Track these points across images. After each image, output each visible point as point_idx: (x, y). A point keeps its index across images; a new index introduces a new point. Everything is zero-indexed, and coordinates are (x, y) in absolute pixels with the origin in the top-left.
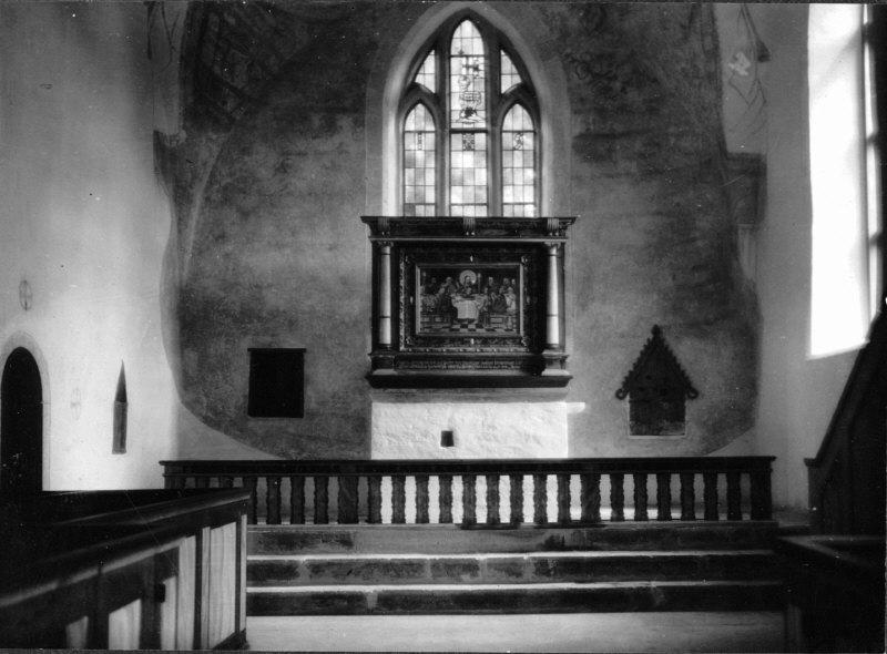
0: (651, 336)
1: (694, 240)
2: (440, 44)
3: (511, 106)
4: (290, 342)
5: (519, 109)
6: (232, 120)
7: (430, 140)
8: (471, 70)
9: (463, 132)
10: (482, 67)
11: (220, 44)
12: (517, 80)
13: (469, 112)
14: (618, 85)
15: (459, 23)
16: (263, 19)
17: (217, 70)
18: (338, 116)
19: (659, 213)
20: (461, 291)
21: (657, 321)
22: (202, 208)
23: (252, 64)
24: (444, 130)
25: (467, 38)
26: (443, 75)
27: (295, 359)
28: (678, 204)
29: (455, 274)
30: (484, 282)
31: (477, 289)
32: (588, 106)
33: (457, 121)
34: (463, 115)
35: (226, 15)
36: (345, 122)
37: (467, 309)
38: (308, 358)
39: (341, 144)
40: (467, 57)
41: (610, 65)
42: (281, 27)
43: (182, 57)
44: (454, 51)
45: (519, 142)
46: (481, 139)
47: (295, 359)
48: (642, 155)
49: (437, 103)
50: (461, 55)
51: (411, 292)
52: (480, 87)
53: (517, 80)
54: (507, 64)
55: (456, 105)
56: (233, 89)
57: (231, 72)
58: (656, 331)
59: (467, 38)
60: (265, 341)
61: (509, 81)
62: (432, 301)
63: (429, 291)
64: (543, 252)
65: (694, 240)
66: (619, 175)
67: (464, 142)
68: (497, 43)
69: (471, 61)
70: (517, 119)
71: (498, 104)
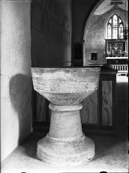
2: (112, 18)
5: (121, 25)
7: (111, 29)
13: (115, 25)
20: (115, 47)
25: (115, 17)
26: (112, 21)
27: (96, 54)
29: (115, 45)
30: (118, 45)
31: (117, 46)
36: (101, 28)
37: (116, 48)
38: (97, 54)
44: (114, 18)
46: (117, 29)
49: (112, 25)
51: (110, 47)
52: (117, 22)
55: (114, 25)
59: (115, 17)
61: (120, 21)
62: (112, 48)
63: (112, 47)
64: (125, 42)
68: (119, 18)
71: (119, 24)
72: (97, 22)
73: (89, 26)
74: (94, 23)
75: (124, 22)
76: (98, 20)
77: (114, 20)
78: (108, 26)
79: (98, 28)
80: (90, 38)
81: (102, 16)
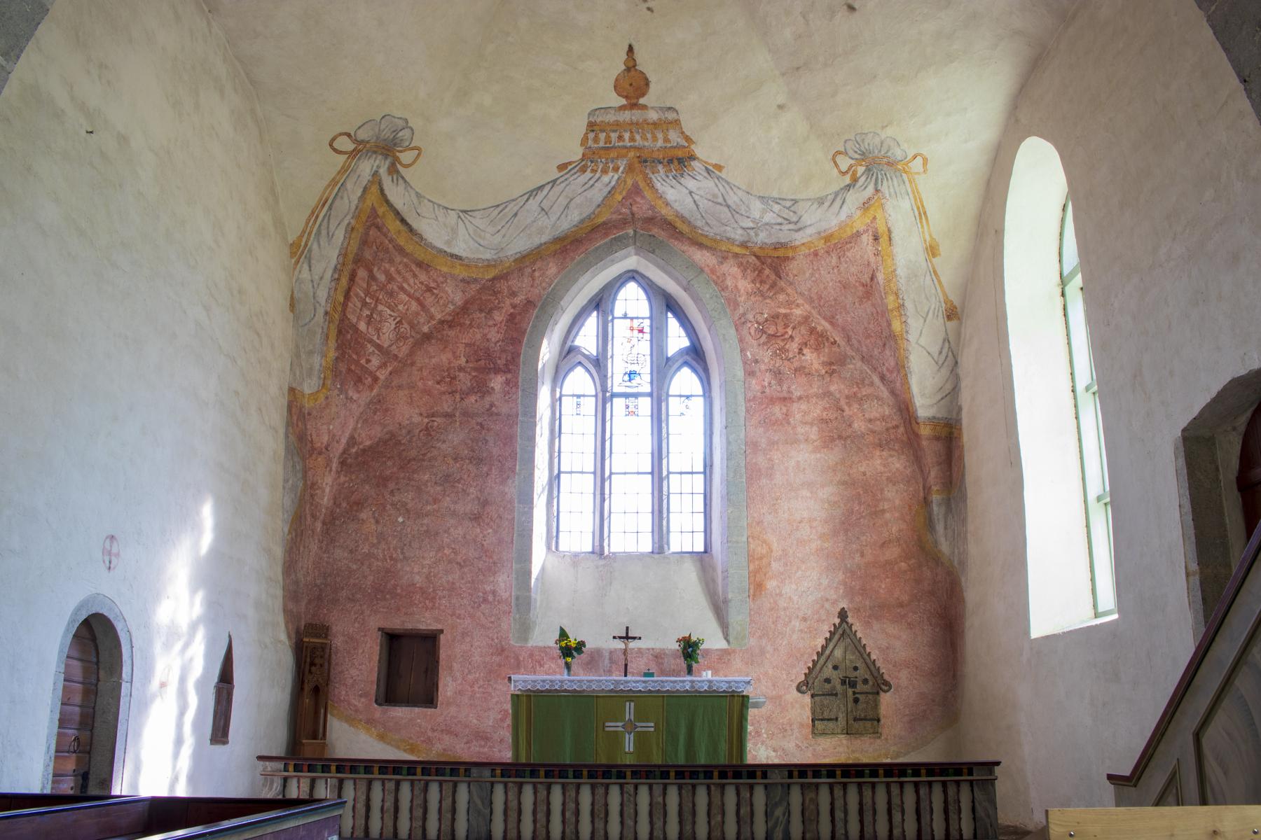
0: (837, 621)
1: (883, 511)
2: (601, 303)
3: (679, 369)
4: (424, 622)
5: (686, 371)
6: (376, 379)
7: (589, 405)
8: (636, 332)
9: (626, 396)
10: (647, 329)
11: (368, 300)
12: (685, 343)
13: (631, 375)
14: (794, 346)
15: (623, 284)
16: (415, 276)
17: (362, 326)
18: (492, 376)
19: (844, 483)
21: (844, 604)
22: (338, 472)
23: (400, 322)
24: (605, 397)
26: (604, 337)
27: (430, 640)
28: (864, 474)
32: (763, 367)
33: (617, 383)
34: (627, 378)
35: (375, 269)
36: (497, 382)
39: (492, 406)
40: (632, 319)
41: (786, 326)
42: (432, 285)
43: (326, 313)
44: (618, 312)
45: (687, 407)
46: (645, 404)
47: (430, 640)
48: (823, 421)
50: (625, 317)
52: (644, 347)
53: (685, 343)
54: (673, 323)
55: (617, 369)
56: (379, 347)
57: (378, 330)
58: (843, 615)
60: (397, 623)
61: (677, 339)
65: (883, 511)
66: (796, 441)
67: (627, 407)
69: (636, 323)
70: (685, 381)
71: (663, 368)
72: (451, 324)
73: (375, 362)
74: (427, 337)
75: (708, 345)
76: (465, 309)
77: (620, 329)
78: (559, 375)
79: (465, 381)
80: (383, 481)
81: (504, 277)
